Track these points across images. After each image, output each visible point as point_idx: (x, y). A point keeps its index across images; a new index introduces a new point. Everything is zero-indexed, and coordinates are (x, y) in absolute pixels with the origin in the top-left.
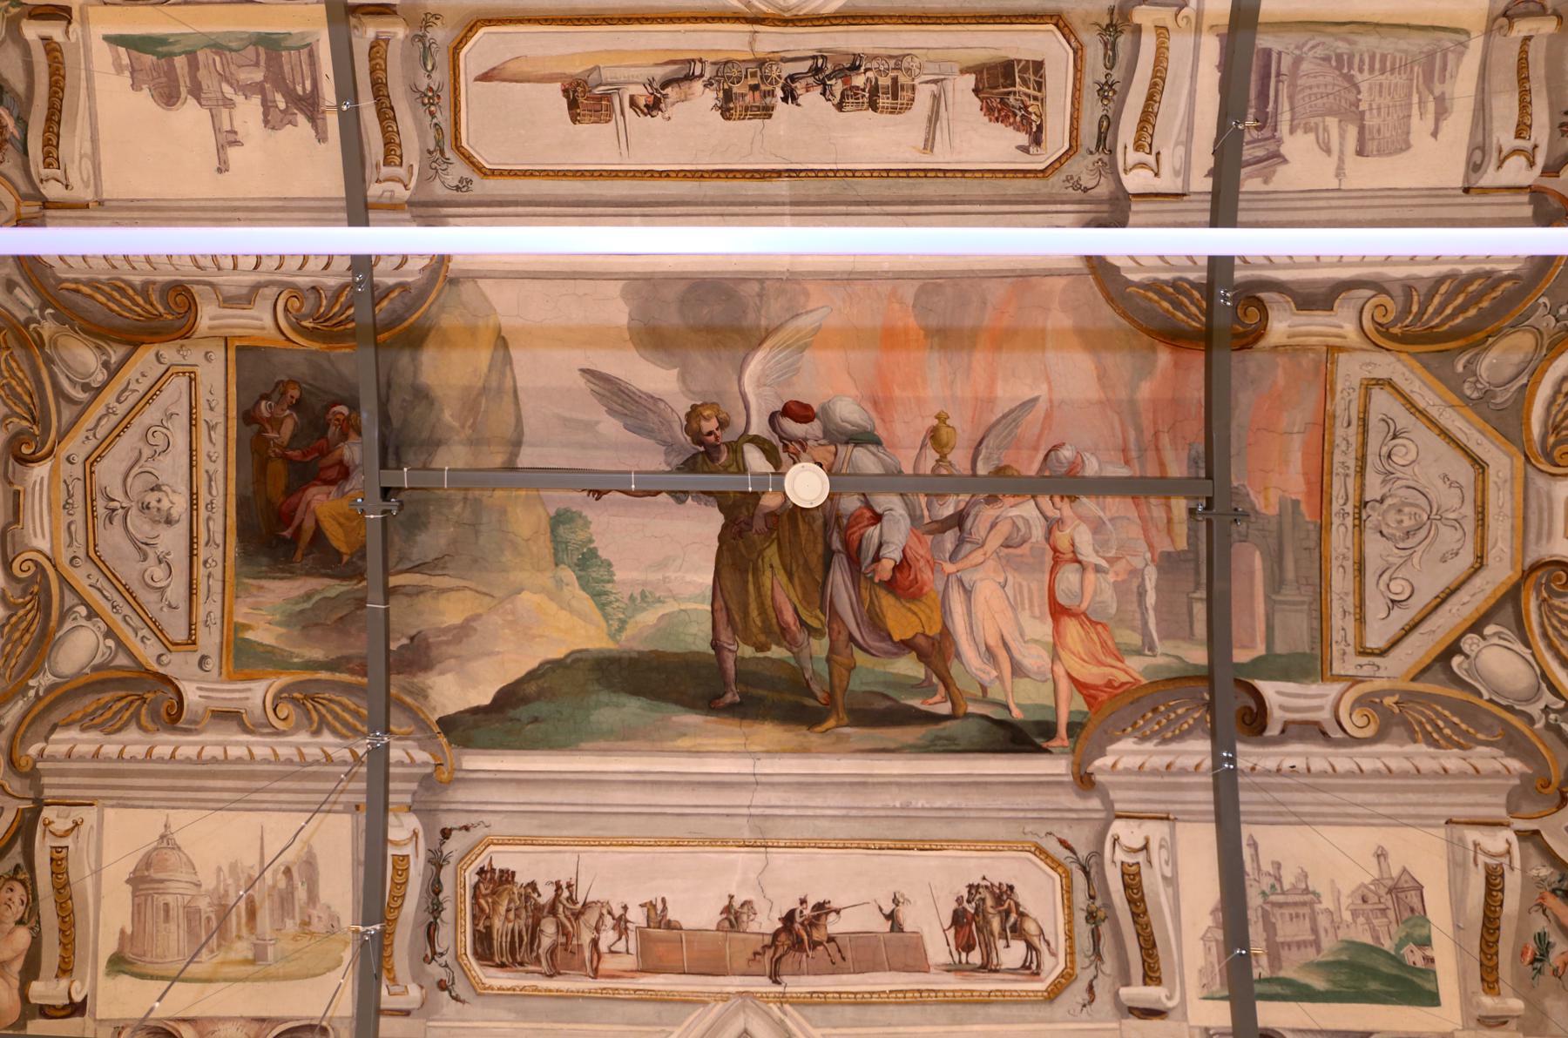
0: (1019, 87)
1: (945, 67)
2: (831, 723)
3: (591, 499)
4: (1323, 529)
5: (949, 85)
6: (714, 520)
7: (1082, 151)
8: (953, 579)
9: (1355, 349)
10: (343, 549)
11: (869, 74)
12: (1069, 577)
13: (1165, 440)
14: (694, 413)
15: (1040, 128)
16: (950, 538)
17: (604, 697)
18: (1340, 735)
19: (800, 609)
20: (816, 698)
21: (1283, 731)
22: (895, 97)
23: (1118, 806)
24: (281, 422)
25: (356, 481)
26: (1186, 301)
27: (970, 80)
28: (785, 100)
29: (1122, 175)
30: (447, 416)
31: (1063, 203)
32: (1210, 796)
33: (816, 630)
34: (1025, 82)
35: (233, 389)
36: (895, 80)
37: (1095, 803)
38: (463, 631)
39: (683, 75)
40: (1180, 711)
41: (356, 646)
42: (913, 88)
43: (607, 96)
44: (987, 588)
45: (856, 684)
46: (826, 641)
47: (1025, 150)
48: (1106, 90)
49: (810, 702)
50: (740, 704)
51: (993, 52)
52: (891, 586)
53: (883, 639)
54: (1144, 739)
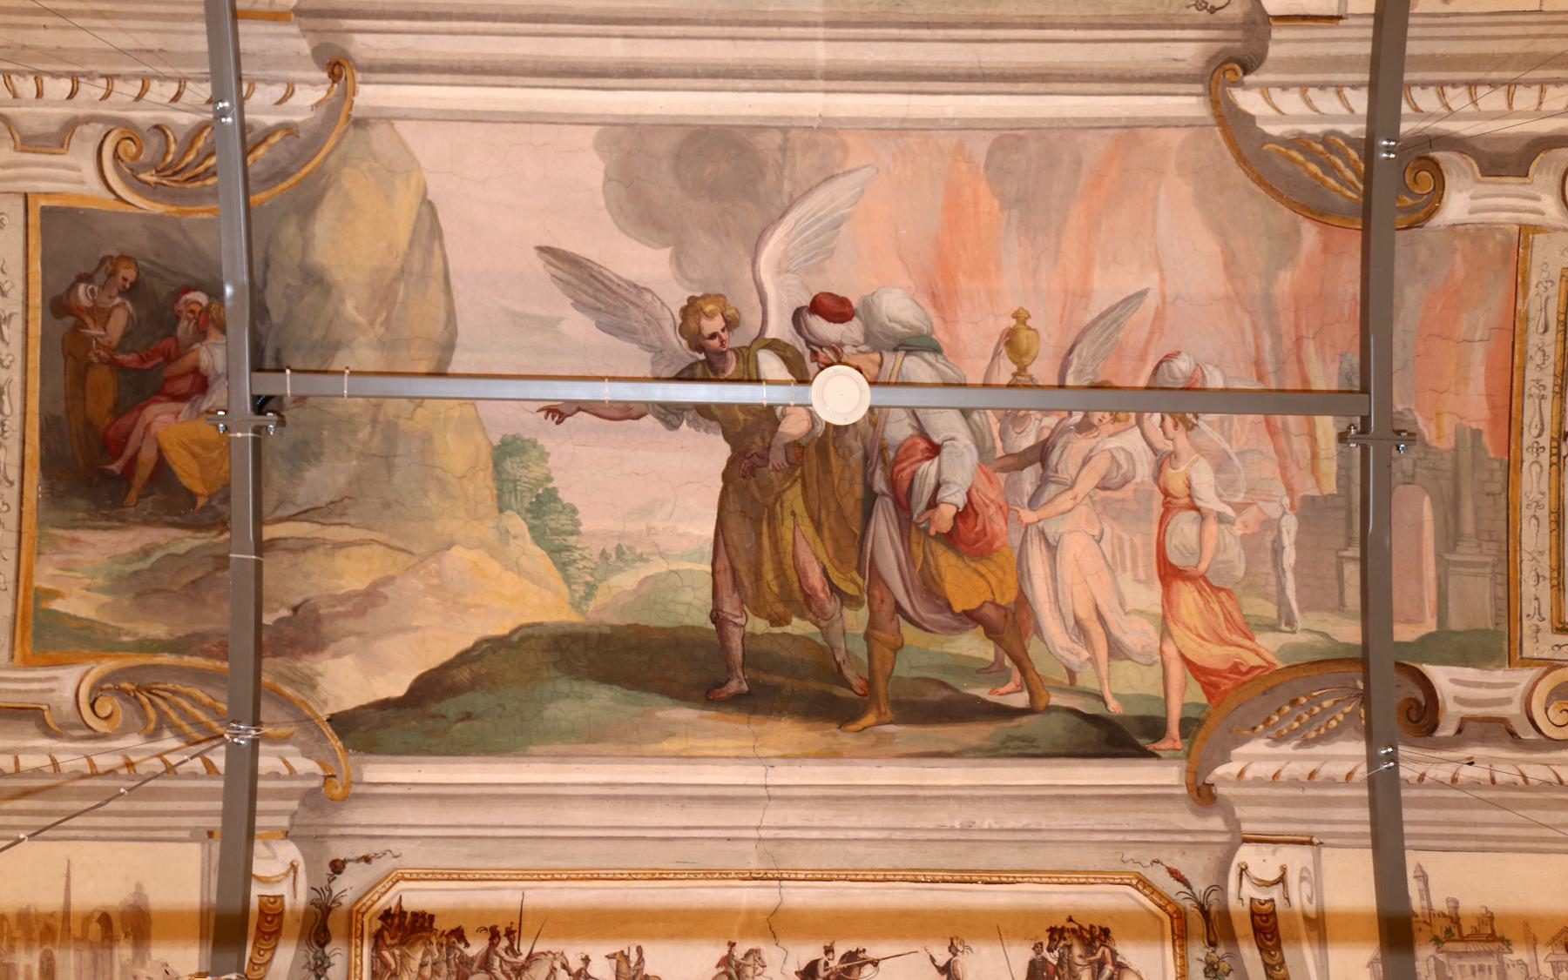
2: (870, 719)
3: (550, 422)
4: (1512, 468)
6: (714, 452)
8: (1033, 531)
9: (1556, 229)
10: (198, 488)
12: (1184, 527)
13: (1310, 349)
14: (692, 309)
16: (1029, 476)
17: (563, 685)
18: (1532, 736)
19: (831, 571)
20: (849, 686)
21: (1459, 731)
23: (1246, 827)
24: (109, 314)
25: (216, 397)
26: (1339, 162)
30: (349, 308)
31: (1183, 27)
32: (1364, 814)
33: (851, 598)
35: (36, 267)
37: (1216, 822)
38: (369, 599)
40: (1326, 704)
41: (214, 619)
44: (1077, 547)
45: (902, 669)
46: (864, 613)
49: (841, 692)
50: (749, 693)
52: (950, 539)
53: (940, 610)
54: (1279, 739)
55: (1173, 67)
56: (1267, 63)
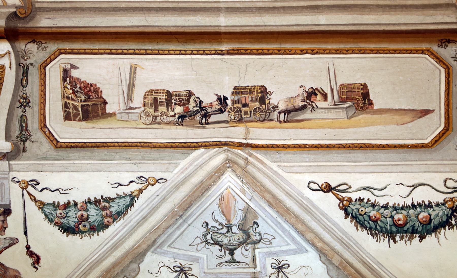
0: (79, 104)
1: (125, 117)
5: (123, 106)
7: (37, 66)
11: (172, 113)
15: (64, 80)
22: (156, 100)
27: (109, 109)
28: (226, 98)
29: (11, 50)
34: (75, 107)
36: (156, 110)
39: (291, 114)
42: (144, 105)
43: (342, 100)
47: (73, 67)
48: (25, 103)
51: (96, 125)
55: (51, 15)
56: (5, 17)
